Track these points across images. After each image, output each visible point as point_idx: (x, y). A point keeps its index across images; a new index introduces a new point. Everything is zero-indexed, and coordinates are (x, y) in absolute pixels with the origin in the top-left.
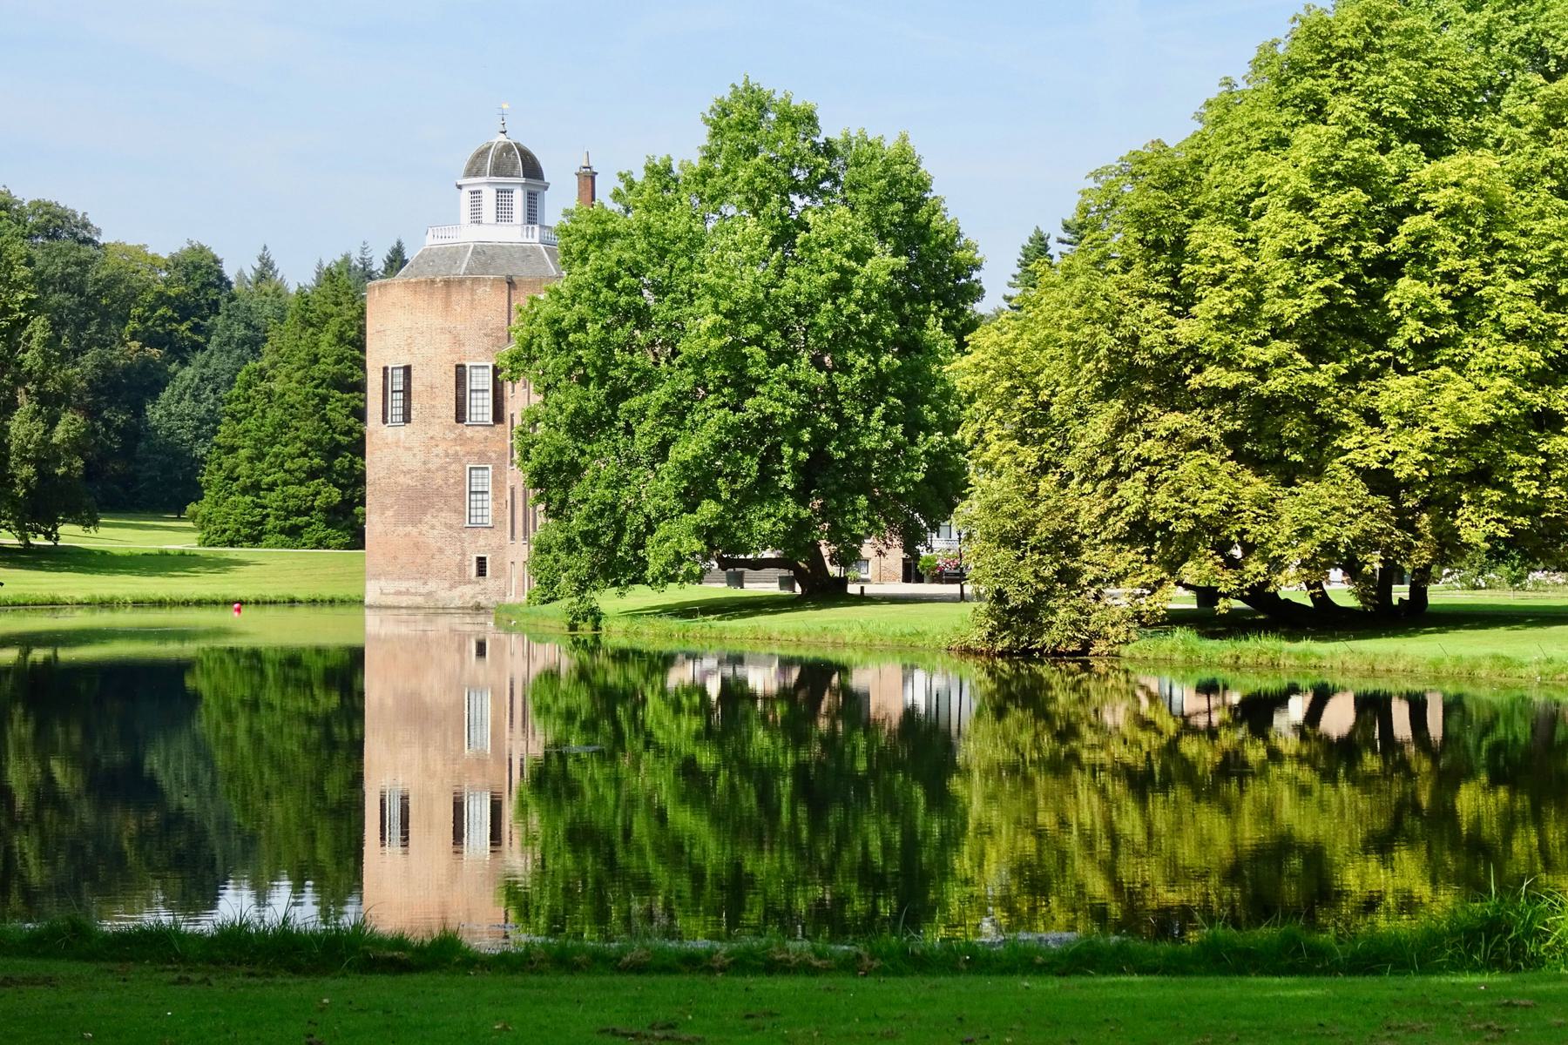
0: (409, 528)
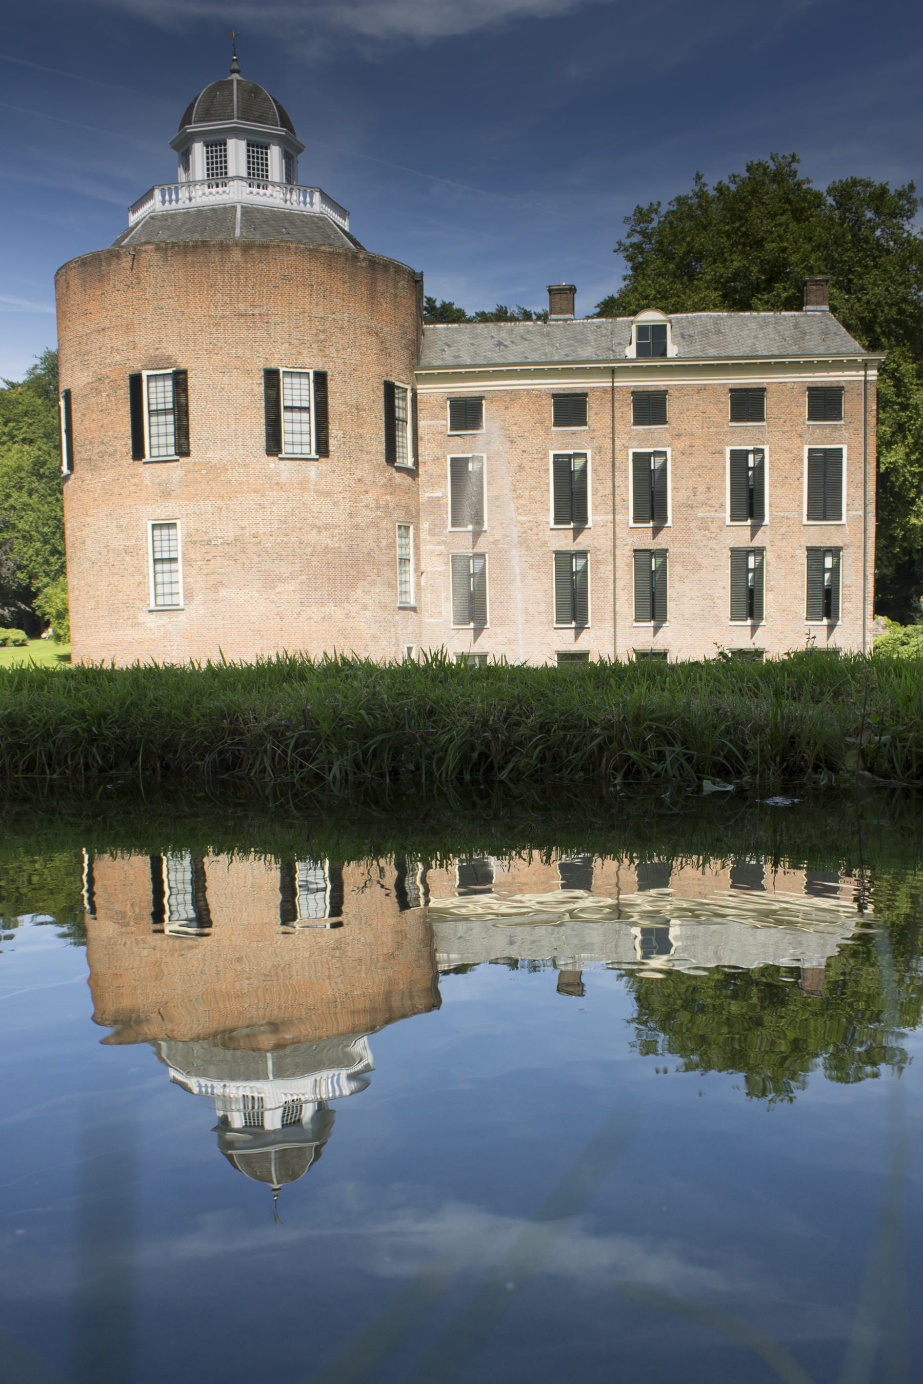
0: (330, 608)
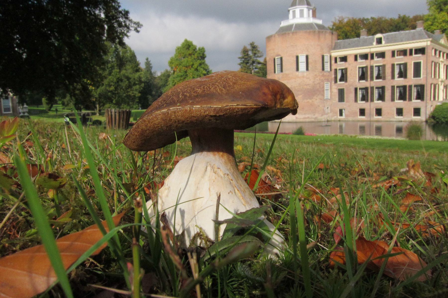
0: (309, 100)
